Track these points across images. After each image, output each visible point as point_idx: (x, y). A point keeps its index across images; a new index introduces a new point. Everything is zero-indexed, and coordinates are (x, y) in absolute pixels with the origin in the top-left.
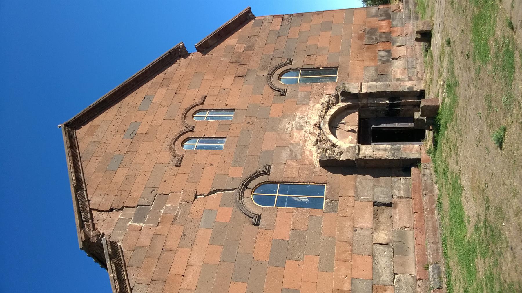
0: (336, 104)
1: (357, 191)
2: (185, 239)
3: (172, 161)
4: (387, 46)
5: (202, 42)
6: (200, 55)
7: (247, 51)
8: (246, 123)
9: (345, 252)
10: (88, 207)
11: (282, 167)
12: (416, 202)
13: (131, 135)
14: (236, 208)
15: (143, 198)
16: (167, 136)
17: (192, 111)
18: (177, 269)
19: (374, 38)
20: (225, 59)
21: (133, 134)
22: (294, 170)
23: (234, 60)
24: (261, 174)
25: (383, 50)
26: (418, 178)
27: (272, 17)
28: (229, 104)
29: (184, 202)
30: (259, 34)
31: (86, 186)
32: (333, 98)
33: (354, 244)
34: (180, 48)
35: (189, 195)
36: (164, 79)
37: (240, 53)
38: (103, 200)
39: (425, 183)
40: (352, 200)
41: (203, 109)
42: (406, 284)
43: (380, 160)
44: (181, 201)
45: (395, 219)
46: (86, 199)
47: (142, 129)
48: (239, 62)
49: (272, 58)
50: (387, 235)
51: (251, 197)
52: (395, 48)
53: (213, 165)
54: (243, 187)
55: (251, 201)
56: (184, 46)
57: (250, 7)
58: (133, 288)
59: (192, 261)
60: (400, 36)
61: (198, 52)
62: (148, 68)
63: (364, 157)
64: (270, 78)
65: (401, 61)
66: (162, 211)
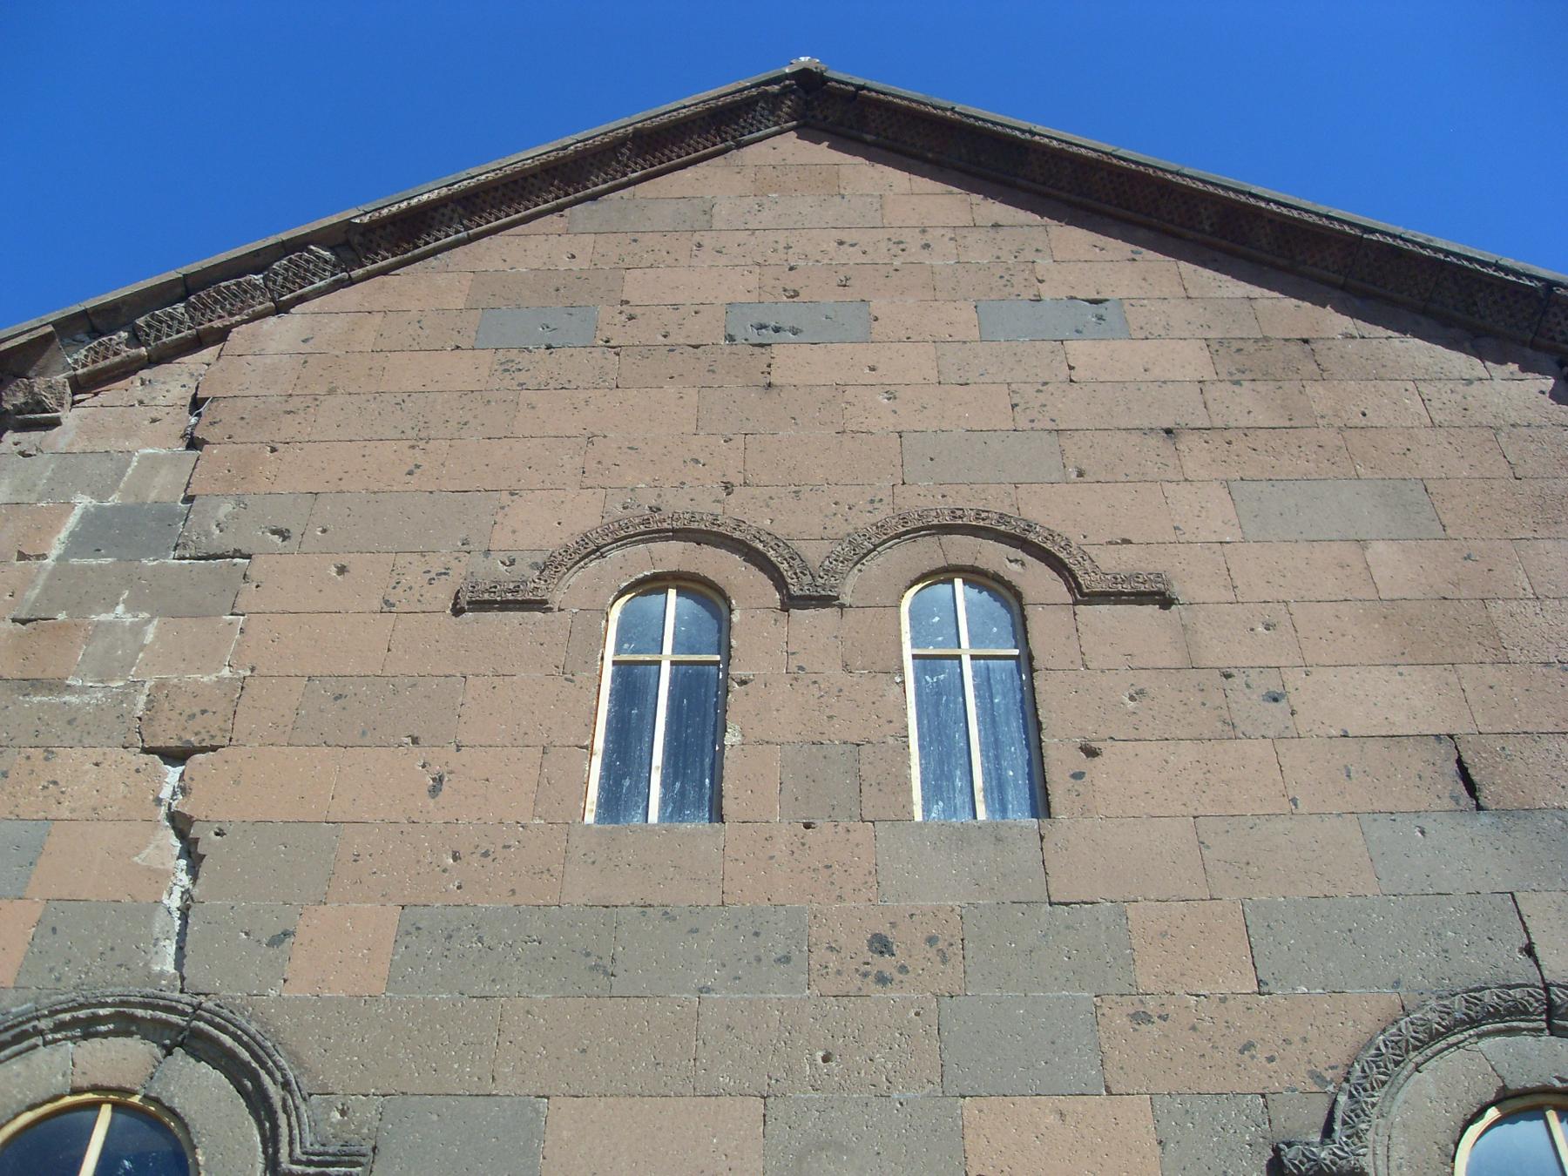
8: (884, 929)
10: (237, 318)
13: (762, 327)
24: (275, 1127)
29: (149, 702)
31: (384, 272)
44: (160, 685)
51: (76, 1091)
53: (435, 791)
54: (175, 1018)
55: (31, 1097)
64: (1495, 1014)
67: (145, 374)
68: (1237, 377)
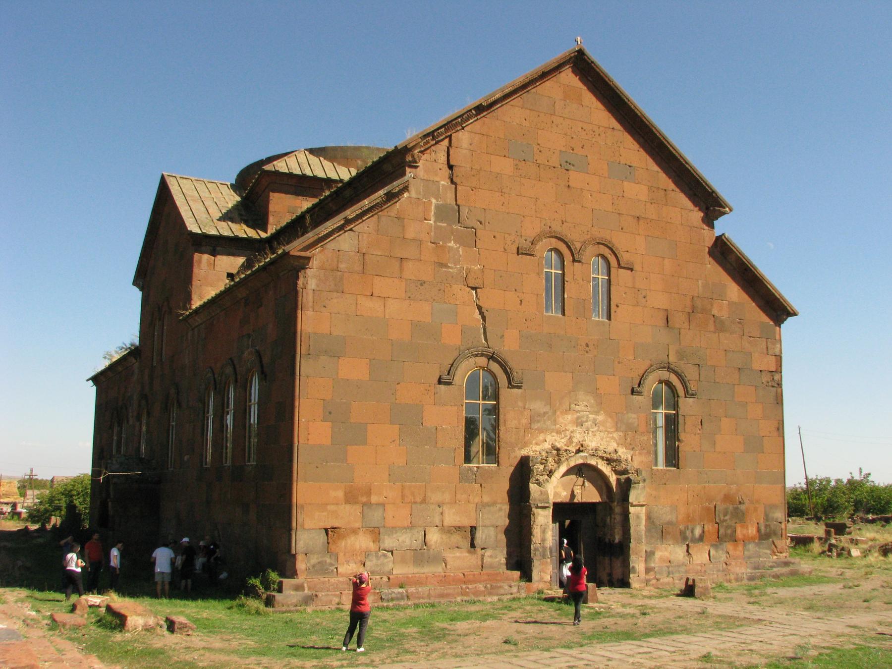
1: (489, 506)
2: (417, 286)
3: (526, 240)
5: (730, 246)
6: (710, 242)
7: (714, 322)
9: (413, 494)
11: (520, 404)
12: (476, 576)
13: (567, 162)
14: (462, 348)
15: (470, 210)
16: (566, 222)
17: (607, 253)
18: (381, 285)
19: (726, 518)
20: (700, 288)
21: (567, 166)
22: (516, 422)
23: (699, 303)
25: (703, 532)
26: (508, 579)
27: (777, 354)
28: (618, 310)
30: (744, 337)
32: (624, 466)
33: (423, 505)
34: (721, 209)
35: (475, 279)
36: (665, 190)
37: (711, 310)
38: (464, 151)
39: (500, 587)
40: (477, 500)
41: (612, 269)
42: (383, 564)
43: (529, 533)
44: (467, 269)
45: (455, 552)
46: (464, 125)
47: (576, 178)
48: (695, 311)
49: (699, 365)
50: (436, 542)
53: (521, 304)
56: (724, 213)
57: (796, 315)
58: (353, 231)
59: (390, 302)
60: (727, 555)
61: (714, 239)
62: (684, 162)
63: (534, 514)
65: (684, 556)
66: (452, 244)
67: (433, 148)
68: (652, 201)
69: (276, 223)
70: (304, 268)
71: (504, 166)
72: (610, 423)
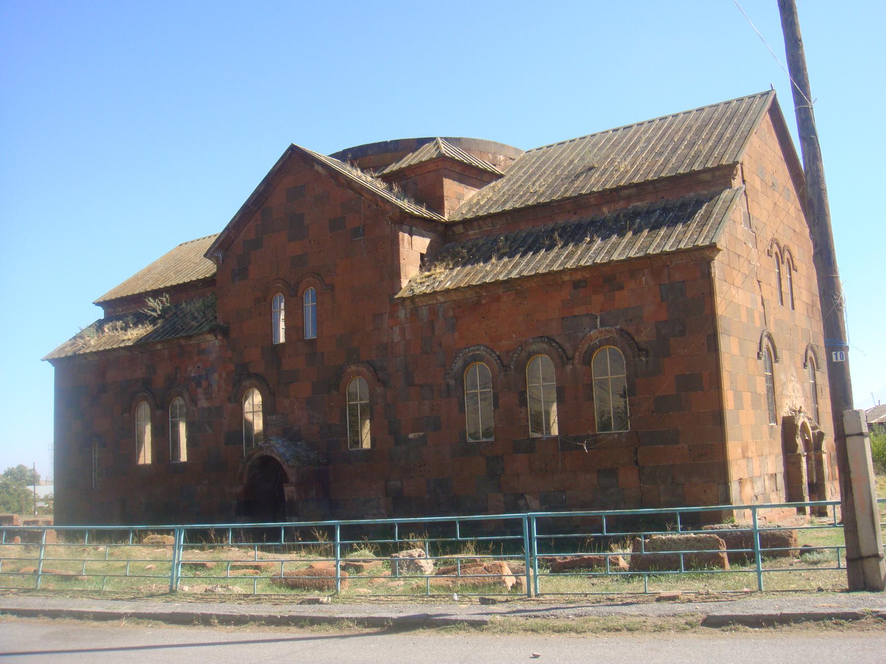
0: (811, 427)
4: (831, 477)
13: (773, 183)
17: (789, 257)
38: (747, 169)
52: (830, 485)
66: (750, 245)
69: (449, 208)
70: (713, 259)
71: (758, 184)
72: (801, 391)
